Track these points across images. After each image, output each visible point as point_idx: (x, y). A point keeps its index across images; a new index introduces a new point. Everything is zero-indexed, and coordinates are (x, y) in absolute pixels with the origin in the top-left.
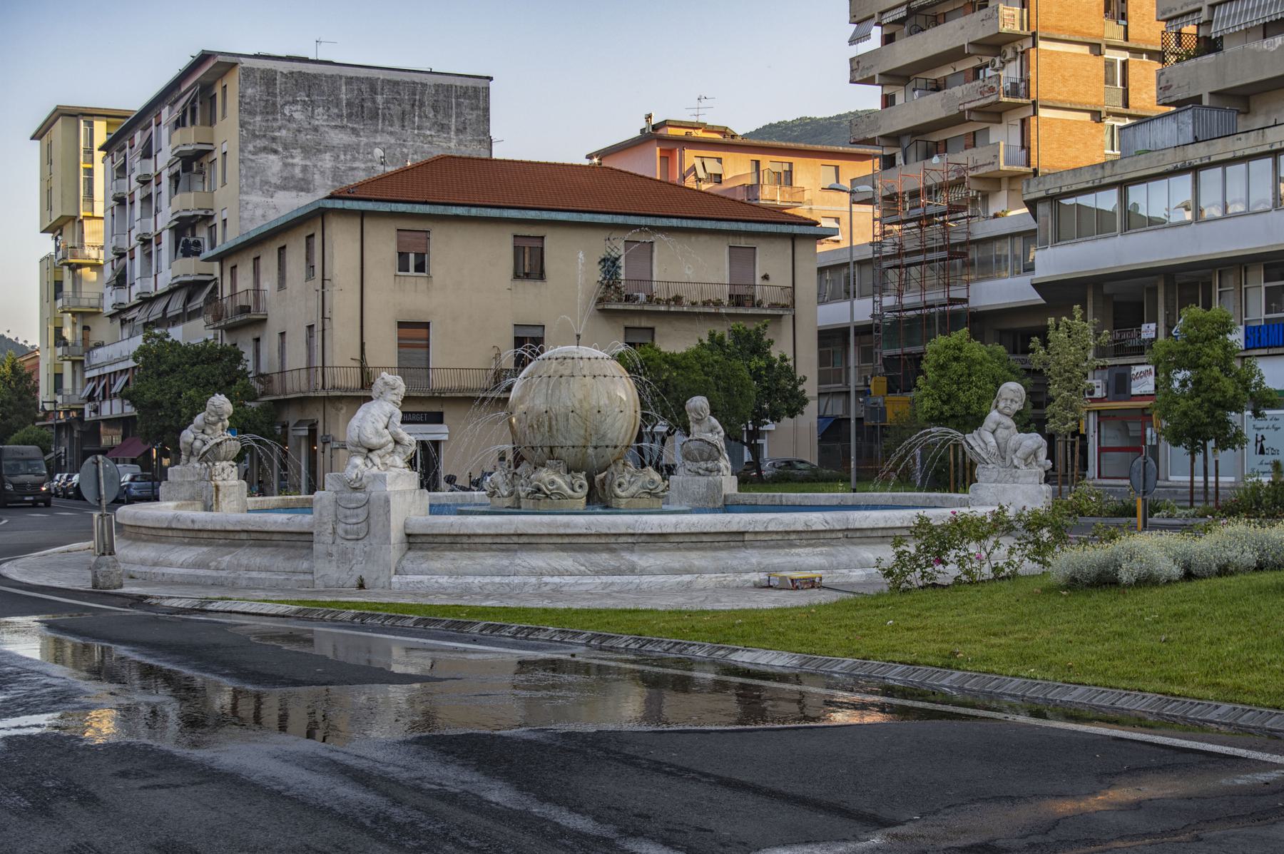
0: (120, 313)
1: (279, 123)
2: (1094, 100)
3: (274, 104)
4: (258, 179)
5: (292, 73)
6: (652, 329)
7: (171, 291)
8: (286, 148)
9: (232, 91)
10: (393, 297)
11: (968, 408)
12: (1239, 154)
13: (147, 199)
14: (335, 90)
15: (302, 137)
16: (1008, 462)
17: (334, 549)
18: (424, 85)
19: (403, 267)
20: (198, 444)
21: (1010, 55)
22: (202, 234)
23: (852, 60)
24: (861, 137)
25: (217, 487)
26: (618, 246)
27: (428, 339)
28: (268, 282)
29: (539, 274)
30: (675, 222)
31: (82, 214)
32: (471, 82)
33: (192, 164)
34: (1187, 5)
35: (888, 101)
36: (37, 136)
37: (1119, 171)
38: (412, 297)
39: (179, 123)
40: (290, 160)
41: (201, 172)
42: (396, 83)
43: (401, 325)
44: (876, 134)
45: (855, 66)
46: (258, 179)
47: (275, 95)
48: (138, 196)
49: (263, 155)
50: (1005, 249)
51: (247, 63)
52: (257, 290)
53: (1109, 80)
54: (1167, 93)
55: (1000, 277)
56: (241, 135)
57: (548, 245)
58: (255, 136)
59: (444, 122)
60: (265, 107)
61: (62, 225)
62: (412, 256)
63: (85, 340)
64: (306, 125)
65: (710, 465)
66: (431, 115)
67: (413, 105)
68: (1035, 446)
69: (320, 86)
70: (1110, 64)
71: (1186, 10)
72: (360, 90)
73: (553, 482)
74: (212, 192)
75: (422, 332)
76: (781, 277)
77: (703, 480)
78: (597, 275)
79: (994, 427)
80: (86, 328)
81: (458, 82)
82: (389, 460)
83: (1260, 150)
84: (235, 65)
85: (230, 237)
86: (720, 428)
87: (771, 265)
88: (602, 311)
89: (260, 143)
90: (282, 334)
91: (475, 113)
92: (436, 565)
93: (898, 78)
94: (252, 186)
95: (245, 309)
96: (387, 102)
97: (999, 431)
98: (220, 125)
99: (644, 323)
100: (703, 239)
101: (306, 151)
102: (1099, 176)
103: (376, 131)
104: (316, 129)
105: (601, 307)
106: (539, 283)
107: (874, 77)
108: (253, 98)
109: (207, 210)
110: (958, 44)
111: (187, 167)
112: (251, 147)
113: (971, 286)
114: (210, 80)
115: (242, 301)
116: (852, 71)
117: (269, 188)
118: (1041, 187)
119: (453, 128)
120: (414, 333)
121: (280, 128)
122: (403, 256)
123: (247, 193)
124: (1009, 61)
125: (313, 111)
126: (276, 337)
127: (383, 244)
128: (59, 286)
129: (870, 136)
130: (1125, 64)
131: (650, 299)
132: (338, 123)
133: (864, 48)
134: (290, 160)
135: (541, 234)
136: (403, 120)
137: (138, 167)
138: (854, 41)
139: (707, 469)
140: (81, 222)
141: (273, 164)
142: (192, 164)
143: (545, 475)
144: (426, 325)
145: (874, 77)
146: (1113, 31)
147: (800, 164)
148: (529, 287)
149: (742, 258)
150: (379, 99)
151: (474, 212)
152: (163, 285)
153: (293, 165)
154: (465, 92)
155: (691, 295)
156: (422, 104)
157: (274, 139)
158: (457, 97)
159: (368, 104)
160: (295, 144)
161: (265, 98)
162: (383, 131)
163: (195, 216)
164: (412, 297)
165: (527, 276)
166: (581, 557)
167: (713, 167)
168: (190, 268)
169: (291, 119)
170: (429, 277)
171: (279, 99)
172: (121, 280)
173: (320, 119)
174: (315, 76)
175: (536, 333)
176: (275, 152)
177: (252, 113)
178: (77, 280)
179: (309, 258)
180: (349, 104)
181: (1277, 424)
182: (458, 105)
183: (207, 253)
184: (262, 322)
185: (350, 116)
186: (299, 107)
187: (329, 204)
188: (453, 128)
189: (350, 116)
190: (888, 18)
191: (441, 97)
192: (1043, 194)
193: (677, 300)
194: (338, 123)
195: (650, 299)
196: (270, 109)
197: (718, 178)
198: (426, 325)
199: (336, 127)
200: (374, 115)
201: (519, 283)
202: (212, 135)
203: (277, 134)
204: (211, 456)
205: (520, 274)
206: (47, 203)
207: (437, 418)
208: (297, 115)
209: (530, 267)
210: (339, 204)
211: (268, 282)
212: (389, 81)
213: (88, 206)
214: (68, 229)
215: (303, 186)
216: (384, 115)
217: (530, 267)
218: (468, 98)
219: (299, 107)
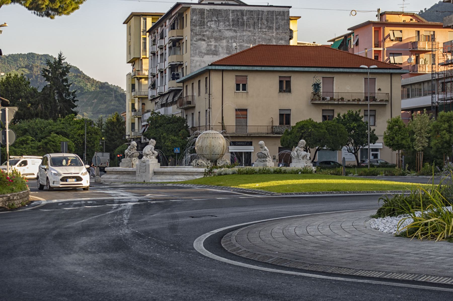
0: (154, 99)
1: (206, 29)
3: (204, 22)
4: (197, 51)
5: (211, 10)
6: (333, 110)
7: (169, 93)
8: (208, 39)
9: (188, 16)
10: (233, 100)
11: (398, 142)
13: (162, 55)
14: (227, 16)
15: (215, 34)
17: (139, 175)
18: (263, 11)
19: (238, 89)
20: (129, 153)
22: (180, 71)
24: (446, 25)
25: (133, 164)
26: (319, 79)
27: (247, 115)
28: (196, 94)
29: (289, 90)
30: (341, 70)
31: (142, 56)
32: (282, 9)
33: (176, 43)
36: (126, 22)
38: (242, 100)
39: (173, 27)
40: (210, 43)
41: (180, 47)
42: (252, 11)
43: (236, 110)
46: (197, 51)
48: (159, 53)
49: (200, 42)
51: (193, 7)
52: (193, 96)
56: (191, 35)
58: (196, 35)
59: (271, 25)
60: (200, 23)
61: (134, 61)
62: (241, 85)
63: (143, 109)
64: (216, 29)
65: (264, 159)
66: (266, 23)
67: (258, 20)
69: (221, 14)
72: (237, 15)
73: (201, 163)
74: (183, 54)
75: (245, 112)
76: (386, 89)
77: (262, 163)
78: (311, 90)
80: (143, 104)
82: (151, 157)
84: (189, 7)
85: (189, 73)
86: (267, 149)
87: (382, 85)
89: (198, 37)
90: (199, 112)
91: (283, 22)
92: (158, 178)
94: (195, 54)
95: (189, 103)
96: (248, 19)
98: (185, 29)
99: (330, 108)
100: (354, 76)
101: (216, 39)
103: (244, 31)
104: (220, 31)
106: (289, 94)
108: (196, 20)
109: (181, 62)
111: (174, 45)
112: (195, 39)
114: (181, 12)
115: (190, 99)
117: (202, 54)
119: (274, 28)
120: (242, 113)
121: (206, 31)
122: (238, 85)
123: (193, 57)
125: (219, 24)
126: (198, 113)
127: (230, 81)
128: (133, 86)
129: (449, 25)
131: (332, 99)
132: (228, 28)
134: (210, 43)
135: (289, 76)
136: (254, 26)
137: (159, 43)
140: (141, 60)
141: (203, 45)
142: (176, 43)
143: (200, 161)
144: (246, 110)
147: (437, 31)
148: (285, 96)
150: (245, 18)
151: (263, 68)
152: (167, 90)
153: (211, 45)
154: (279, 13)
155: (346, 98)
156: (262, 19)
157: (204, 35)
158: (276, 16)
159: (241, 20)
160: (212, 37)
161: (200, 20)
162: (246, 30)
163: (176, 64)
164: (242, 100)
165: (285, 91)
166: (186, 176)
167: (398, 34)
168: (174, 84)
169: (210, 27)
170: (247, 93)
171: (205, 20)
172: (153, 86)
173: (222, 27)
174: (220, 10)
175: (287, 112)
176: (204, 40)
177: (195, 26)
178: (140, 84)
179: (206, 86)
180: (233, 20)
182: (277, 19)
183: (182, 79)
184: (194, 107)
185: (233, 25)
186: (213, 23)
187: (210, 68)
188: (274, 28)
189: (233, 25)
191: (270, 16)
194: (228, 28)
195: (332, 99)
196: (202, 24)
197: (400, 39)
198: (246, 110)
199: (228, 30)
200: (243, 24)
201: (281, 93)
202: (183, 32)
203: (205, 33)
204: (131, 156)
205: (281, 90)
206: (129, 52)
207: (250, 144)
208: (212, 26)
210: (213, 68)
211: (196, 94)
212: (249, 11)
213: (144, 53)
214: (137, 62)
215: (215, 53)
216: (247, 24)
218: (281, 17)
219: (213, 23)
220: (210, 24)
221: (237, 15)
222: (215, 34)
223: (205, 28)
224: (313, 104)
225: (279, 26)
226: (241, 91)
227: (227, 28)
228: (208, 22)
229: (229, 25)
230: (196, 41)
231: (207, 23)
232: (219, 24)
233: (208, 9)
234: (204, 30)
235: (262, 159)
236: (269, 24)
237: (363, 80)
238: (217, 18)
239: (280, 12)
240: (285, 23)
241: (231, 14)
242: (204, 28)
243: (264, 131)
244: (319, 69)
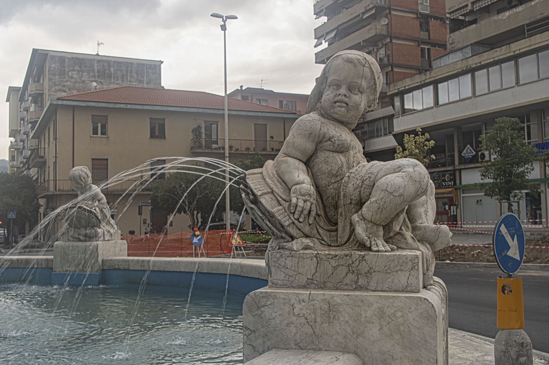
1: (67, 79)
2: (417, 64)
3: (64, 71)
5: (73, 58)
8: (69, 90)
15: (77, 85)
16: (343, 234)
19: (95, 132)
21: (380, 45)
23: (316, 54)
29: (162, 136)
32: (153, 63)
34: (460, 4)
37: (434, 76)
42: (120, 63)
47: (65, 67)
50: (381, 124)
51: (52, 54)
53: (423, 56)
54: (453, 46)
55: (378, 136)
56: (49, 84)
58: (56, 85)
59: (142, 79)
64: (79, 80)
66: (135, 76)
67: (127, 72)
68: (411, 189)
70: (422, 50)
71: (460, 6)
72: (103, 65)
75: (105, 162)
78: (191, 136)
79: (310, 147)
81: (147, 63)
84: (47, 54)
88: (193, 153)
89: (57, 88)
96: (115, 70)
97: (322, 156)
102: (424, 79)
103: (111, 83)
104: (83, 82)
110: (358, 42)
113: (366, 142)
115: (42, 155)
118: (396, 88)
119: (145, 81)
121: (67, 81)
124: (380, 48)
125: (82, 74)
130: (428, 49)
132: (93, 79)
133: (320, 48)
135: (163, 117)
136: (123, 78)
138: (315, 47)
139: (86, 235)
144: (107, 159)
146: (423, 35)
150: (112, 69)
156: (131, 72)
157: (64, 86)
158: (147, 69)
162: (114, 83)
165: (157, 137)
169: (72, 77)
171: (66, 69)
174: (83, 59)
177: (54, 75)
182: (147, 72)
185: (99, 76)
186: (76, 72)
187: (55, 103)
188: (145, 81)
189: (99, 76)
192: (397, 91)
203: (65, 84)
205: (153, 136)
208: (74, 76)
210: (60, 102)
212: (116, 62)
216: (114, 76)
220: (72, 74)
221: (103, 65)
222: (77, 85)
223: (65, 78)
224: (193, 153)
225: (150, 79)
226: (99, 135)
227: (91, 79)
228: (70, 71)
229: (94, 76)
230: (55, 92)
231: (68, 72)
232: (82, 74)
233: (69, 57)
234: (65, 80)
235: (83, 232)
236: (139, 77)
237: (278, 102)
238: (80, 68)
239: (151, 65)
241: (96, 65)
242: (65, 78)
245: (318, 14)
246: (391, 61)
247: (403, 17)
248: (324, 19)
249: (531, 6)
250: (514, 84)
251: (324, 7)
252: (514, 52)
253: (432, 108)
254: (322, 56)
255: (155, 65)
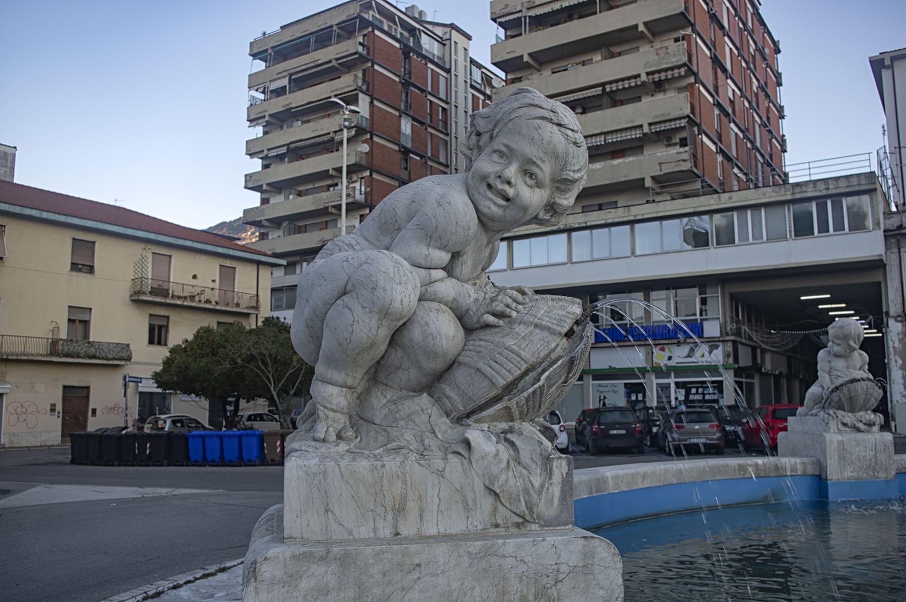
6: (168, 317)
12: (609, 221)
23: (246, 176)
24: (251, 220)
30: (188, 243)
35: (264, 201)
44: (262, 218)
45: (248, 178)
57: (97, 246)
83: (626, 219)
88: (133, 301)
93: (278, 187)
99: (163, 312)
100: (204, 258)
105: (135, 298)
106: (89, 276)
107: (262, 186)
110: (325, 169)
116: (246, 181)
145: (262, 186)
148: (82, 278)
149: (228, 275)
181: (616, 389)
190: (273, 153)
193: (192, 298)
201: (74, 273)
205: (75, 267)
209: (83, 265)
217: (83, 265)
224: (133, 301)
240: (6, 172)
243: (38, 349)
244: (152, 236)
245: (252, 121)
246: (369, 202)
247: (384, 146)
248: (259, 131)
249: (613, 166)
250: (629, 254)
251: (267, 114)
252: (635, 216)
253: (506, 270)
254: (259, 180)
255: (6, 154)
